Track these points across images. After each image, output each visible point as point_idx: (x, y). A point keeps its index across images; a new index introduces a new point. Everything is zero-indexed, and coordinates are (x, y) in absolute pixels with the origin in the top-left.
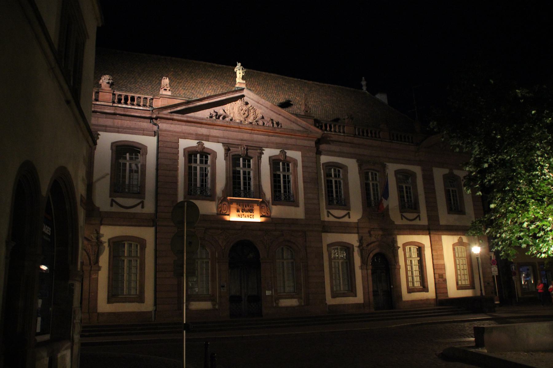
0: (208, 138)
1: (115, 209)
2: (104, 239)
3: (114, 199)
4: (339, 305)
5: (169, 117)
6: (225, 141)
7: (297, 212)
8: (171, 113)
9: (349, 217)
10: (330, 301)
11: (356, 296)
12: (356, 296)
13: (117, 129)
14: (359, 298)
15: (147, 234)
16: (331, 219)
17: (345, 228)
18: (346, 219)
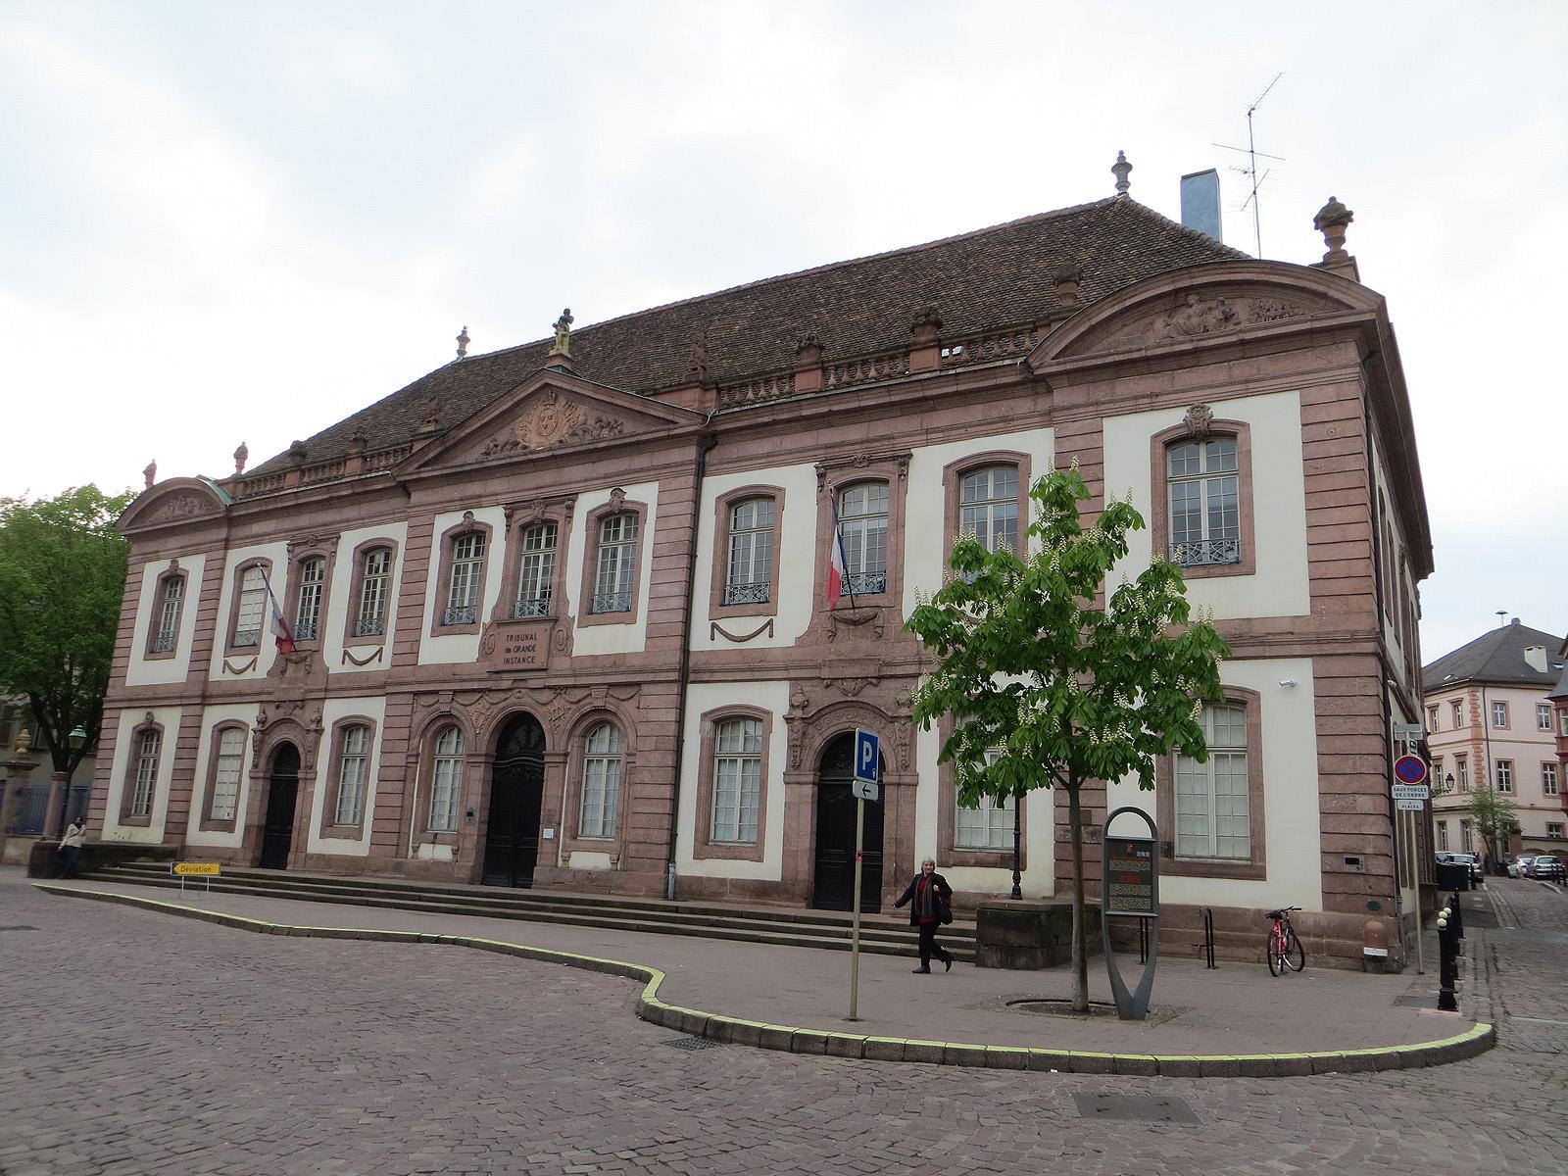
0: (478, 501)
1: (349, 668)
2: (327, 725)
3: (348, 649)
4: (709, 879)
5: (415, 477)
6: (508, 498)
7: (625, 639)
8: (420, 467)
9: (771, 636)
10: (687, 865)
11: (760, 860)
12: (760, 860)
13: (361, 521)
14: (770, 868)
15: (374, 709)
16: (721, 644)
17: (752, 668)
18: (762, 642)
